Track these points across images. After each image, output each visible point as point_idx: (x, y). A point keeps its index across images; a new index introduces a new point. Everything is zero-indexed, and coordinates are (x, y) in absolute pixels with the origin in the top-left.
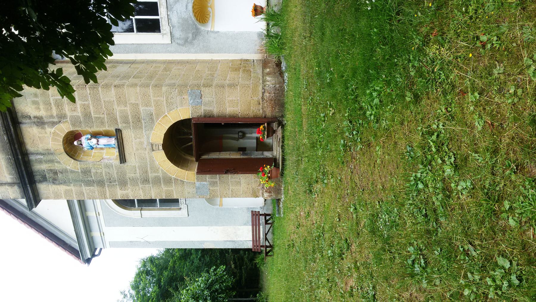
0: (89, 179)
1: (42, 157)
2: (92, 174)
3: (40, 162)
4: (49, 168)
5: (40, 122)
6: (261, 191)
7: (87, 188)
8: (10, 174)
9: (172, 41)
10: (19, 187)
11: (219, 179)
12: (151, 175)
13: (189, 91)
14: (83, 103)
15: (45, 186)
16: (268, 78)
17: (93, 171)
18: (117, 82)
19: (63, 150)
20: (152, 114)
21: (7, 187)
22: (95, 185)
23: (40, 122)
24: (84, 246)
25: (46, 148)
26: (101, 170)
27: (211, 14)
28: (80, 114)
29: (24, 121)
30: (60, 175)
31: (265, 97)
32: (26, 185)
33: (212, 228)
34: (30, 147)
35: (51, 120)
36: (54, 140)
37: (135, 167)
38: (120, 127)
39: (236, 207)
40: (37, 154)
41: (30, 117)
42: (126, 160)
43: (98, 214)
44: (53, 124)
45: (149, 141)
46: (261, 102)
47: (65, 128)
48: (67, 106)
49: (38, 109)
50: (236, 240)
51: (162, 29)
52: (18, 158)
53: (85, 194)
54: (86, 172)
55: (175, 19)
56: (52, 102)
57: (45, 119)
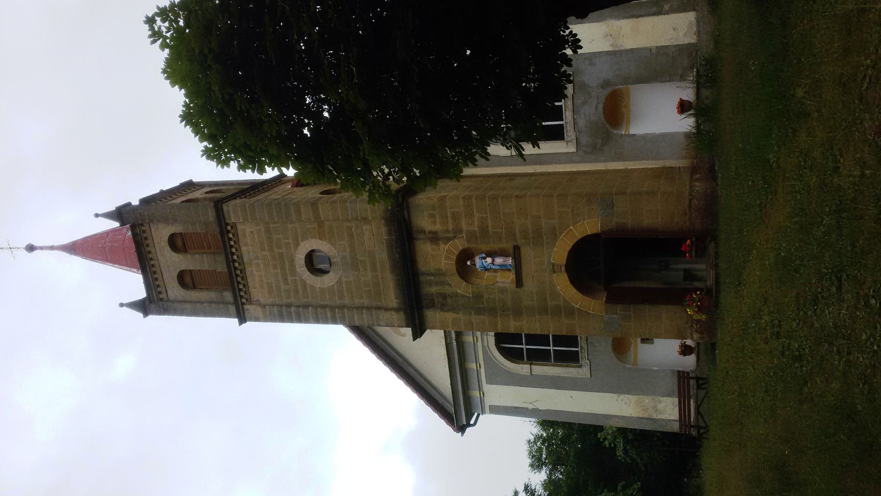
0: (480, 306)
1: (432, 278)
2: (484, 299)
3: (430, 284)
4: (439, 292)
5: (435, 238)
6: (689, 331)
7: (477, 317)
8: (397, 298)
9: (578, 149)
10: (406, 314)
11: (633, 312)
13: (599, 200)
14: (481, 216)
15: (432, 313)
16: (697, 184)
17: (486, 296)
18: (516, 193)
19: (455, 271)
20: (555, 228)
21: (393, 313)
22: (486, 313)
23: (435, 238)
24: (459, 406)
25: (437, 268)
26: (494, 295)
27: (625, 116)
28: (476, 229)
30: (449, 300)
31: (693, 205)
33: (622, 397)
34: (422, 266)
35: (446, 235)
36: (447, 258)
38: (519, 243)
39: (656, 368)
41: (425, 232)
42: (524, 285)
43: (478, 366)
44: (448, 239)
45: (551, 260)
46: (688, 212)
47: (459, 244)
48: (464, 219)
49: (435, 223)
51: (567, 136)
53: (475, 324)
54: (478, 297)
55: (582, 123)
56: (449, 215)
57: (440, 234)
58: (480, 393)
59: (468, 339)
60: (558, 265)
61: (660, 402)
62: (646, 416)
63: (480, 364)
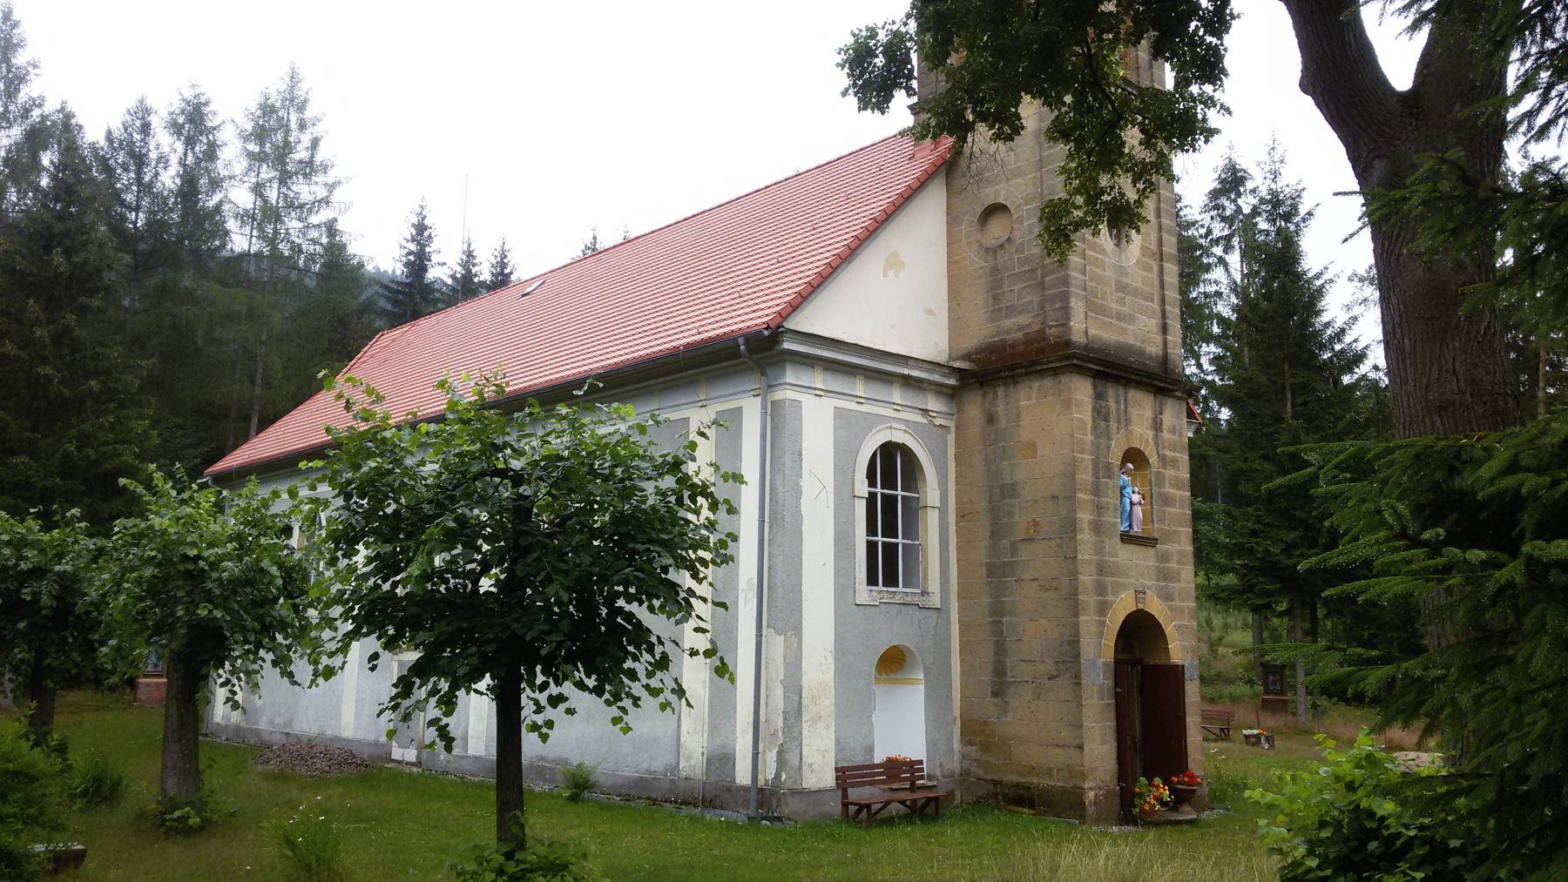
29: (1158, 401)
32: (1104, 366)
33: (831, 660)
34: (1134, 394)
40: (1125, 400)
47: (1153, 460)
50: (804, 719)
52: (1133, 373)
58: (821, 390)
59: (897, 395)
60: (1144, 599)
61: (827, 727)
62: (805, 702)
63: (820, 396)
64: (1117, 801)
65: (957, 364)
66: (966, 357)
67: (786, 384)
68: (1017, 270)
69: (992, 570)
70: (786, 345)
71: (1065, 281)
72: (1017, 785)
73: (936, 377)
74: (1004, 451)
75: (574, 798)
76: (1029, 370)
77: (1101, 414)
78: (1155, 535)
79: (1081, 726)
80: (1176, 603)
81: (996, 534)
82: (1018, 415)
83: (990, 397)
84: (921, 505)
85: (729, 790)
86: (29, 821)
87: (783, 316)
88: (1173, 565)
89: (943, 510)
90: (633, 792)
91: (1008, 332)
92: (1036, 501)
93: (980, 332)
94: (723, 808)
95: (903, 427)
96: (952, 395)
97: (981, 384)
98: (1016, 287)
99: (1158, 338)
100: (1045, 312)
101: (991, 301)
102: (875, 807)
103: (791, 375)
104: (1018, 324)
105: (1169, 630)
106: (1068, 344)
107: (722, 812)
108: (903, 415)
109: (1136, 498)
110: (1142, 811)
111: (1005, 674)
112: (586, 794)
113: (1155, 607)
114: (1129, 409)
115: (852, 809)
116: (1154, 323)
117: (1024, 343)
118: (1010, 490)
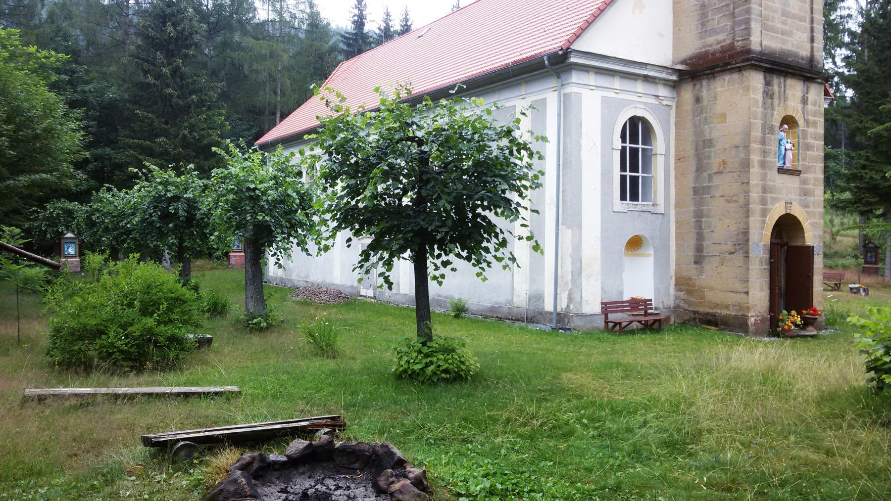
6: (754, 314)
12: (769, 196)
24: (589, 59)
33: (599, 243)
37: (774, 181)
40: (785, 86)
47: (801, 122)
52: (790, 68)
59: (640, 87)
62: (583, 266)
64: (768, 323)
65: (678, 67)
66: (683, 62)
67: (572, 83)
68: (717, 6)
69: (696, 191)
70: (573, 59)
71: (748, 11)
72: (708, 313)
73: (664, 75)
74: (706, 119)
75: (457, 316)
76: (724, 68)
77: (768, 95)
78: (800, 169)
79: (748, 281)
80: (811, 209)
81: (700, 169)
82: (715, 97)
83: (698, 87)
84: (653, 153)
85: (541, 314)
86: (185, 322)
87: (571, 42)
88: (811, 186)
89: (667, 156)
90: (488, 314)
91: (710, 46)
92: (725, 149)
93: (692, 46)
94: (537, 323)
95: (643, 106)
96: (674, 86)
97: (693, 79)
98: (716, 17)
99: (808, 46)
100: (734, 32)
101: (700, 26)
102: (624, 324)
103: (575, 77)
104: (717, 40)
105: (806, 225)
106: (749, 51)
107: (538, 325)
108: (644, 99)
109: (789, 146)
110: (783, 329)
111: (702, 251)
112: (463, 314)
113: (797, 211)
114: (787, 91)
115: (611, 325)
116: (806, 36)
117: (721, 52)
118: (709, 143)
